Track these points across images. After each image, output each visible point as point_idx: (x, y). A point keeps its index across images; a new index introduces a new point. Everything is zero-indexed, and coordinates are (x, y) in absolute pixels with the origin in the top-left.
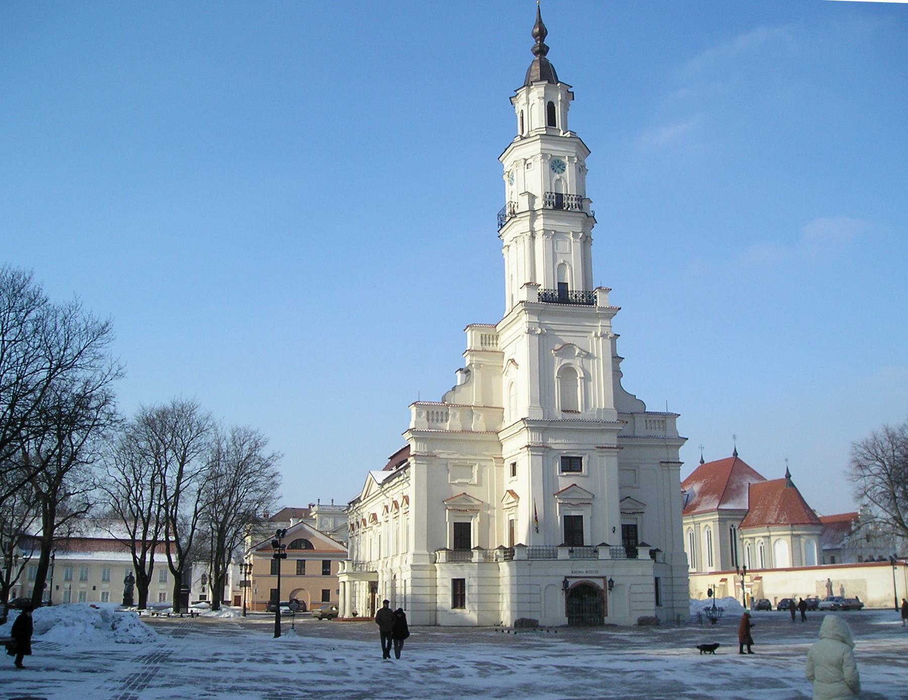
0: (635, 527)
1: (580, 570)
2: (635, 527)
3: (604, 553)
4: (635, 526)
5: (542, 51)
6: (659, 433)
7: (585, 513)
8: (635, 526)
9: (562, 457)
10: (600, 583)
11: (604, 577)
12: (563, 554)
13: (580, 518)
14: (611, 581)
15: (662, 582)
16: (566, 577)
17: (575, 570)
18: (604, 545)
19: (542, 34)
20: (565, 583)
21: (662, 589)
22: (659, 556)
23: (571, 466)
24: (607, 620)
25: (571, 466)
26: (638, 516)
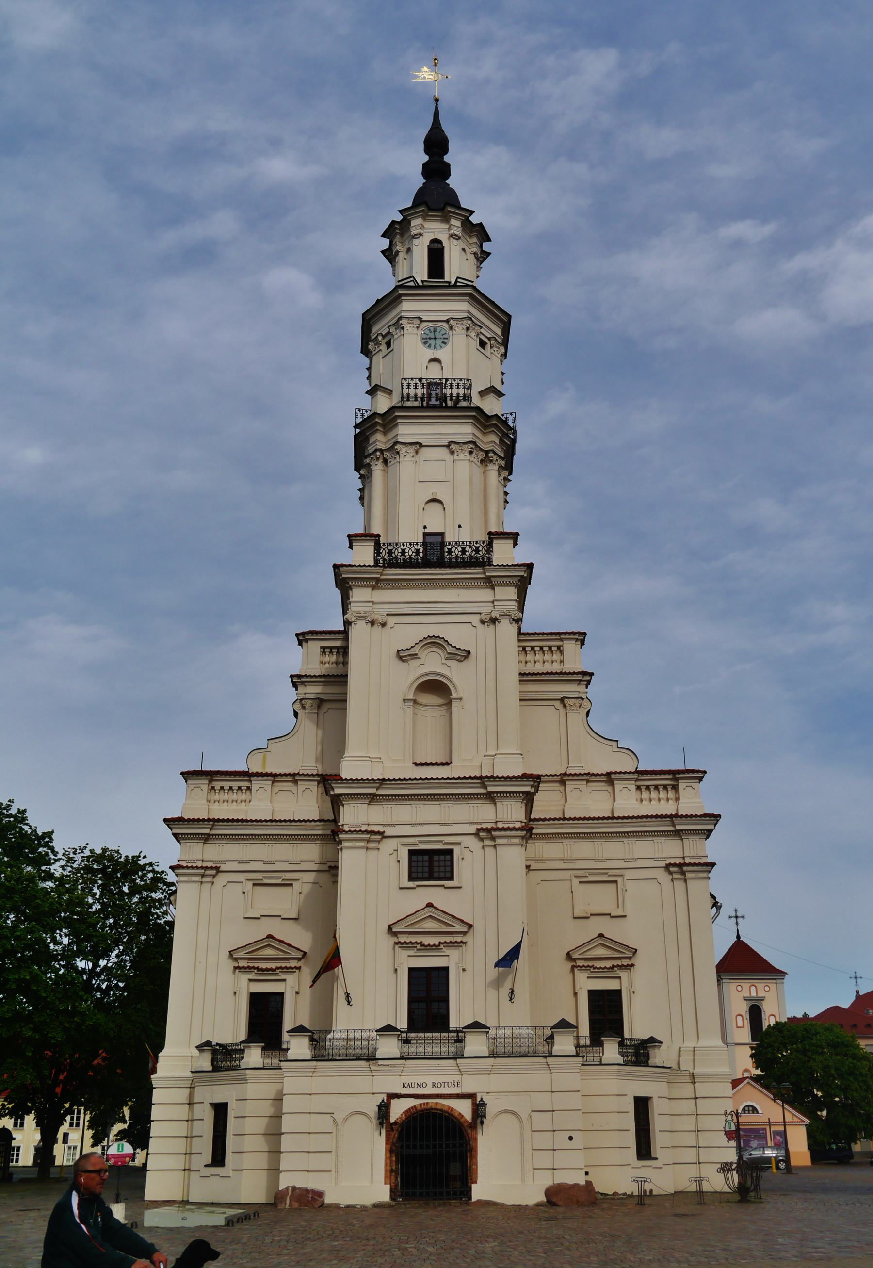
0: (617, 994)
1: (420, 1080)
2: (617, 994)
3: (475, 1044)
4: (618, 993)
5: (436, 170)
6: (668, 808)
7: (449, 959)
8: (619, 992)
9: (411, 853)
10: (464, 1109)
11: (472, 1096)
12: (389, 1047)
13: (446, 969)
14: (483, 1104)
15: (657, 1108)
16: (392, 1096)
17: (407, 1080)
18: (476, 1026)
19: (436, 144)
20: (384, 1110)
21: (658, 1123)
22: (658, 1056)
23: (431, 867)
24: (478, 1192)
25: (431, 867)
26: (624, 975)
